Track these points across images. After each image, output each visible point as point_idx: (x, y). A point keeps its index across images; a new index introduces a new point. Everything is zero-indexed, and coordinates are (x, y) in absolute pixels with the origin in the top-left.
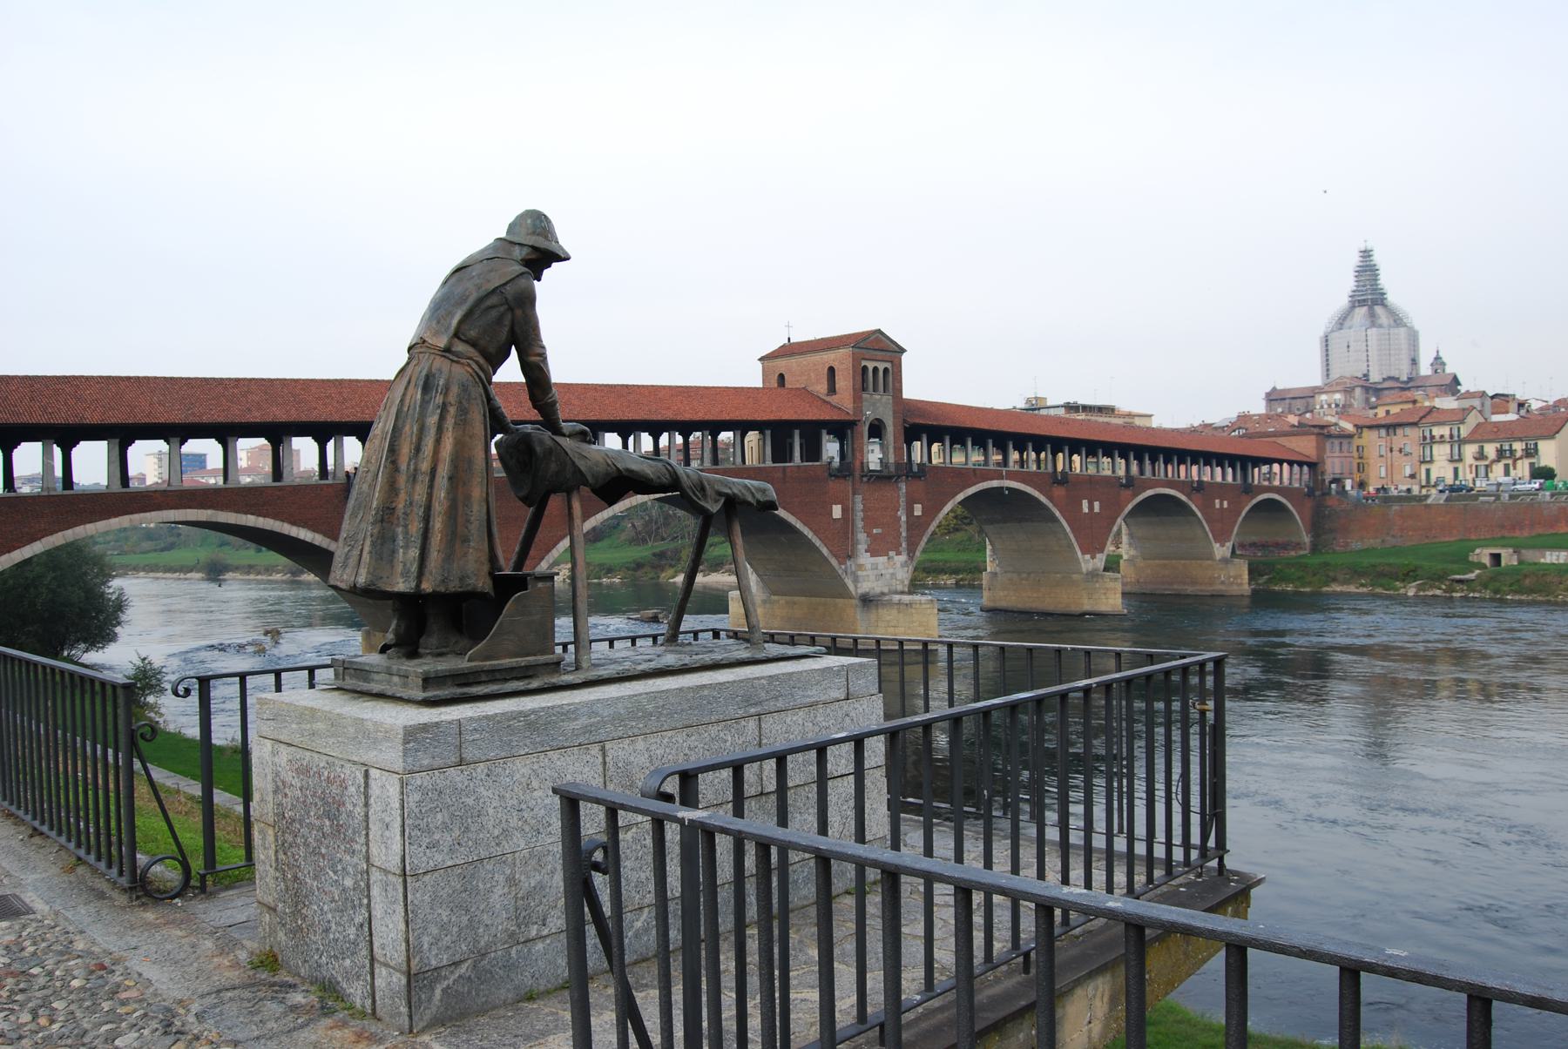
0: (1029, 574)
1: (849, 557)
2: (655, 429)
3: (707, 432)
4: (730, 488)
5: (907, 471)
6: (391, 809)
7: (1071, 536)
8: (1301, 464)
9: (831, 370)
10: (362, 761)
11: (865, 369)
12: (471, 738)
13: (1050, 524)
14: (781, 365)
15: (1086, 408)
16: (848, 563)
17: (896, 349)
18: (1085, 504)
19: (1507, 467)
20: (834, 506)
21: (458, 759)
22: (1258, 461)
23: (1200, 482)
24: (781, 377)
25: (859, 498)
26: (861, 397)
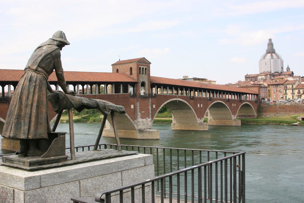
0: (184, 123)
1: (136, 119)
2: (83, 84)
3: (97, 85)
4: (113, 108)
5: (151, 96)
6: (21, 201)
7: (195, 113)
8: (254, 94)
9: (131, 68)
10: (12, 187)
11: (140, 68)
12: (43, 180)
13: (189, 110)
14: (118, 67)
15: (199, 79)
16: (135, 121)
17: (149, 63)
18: (199, 105)
20: (132, 105)
21: (40, 186)
22: (243, 94)
23: (228, 99)
24: (117, 70)
25: (138, 103)
26: (139, 76)
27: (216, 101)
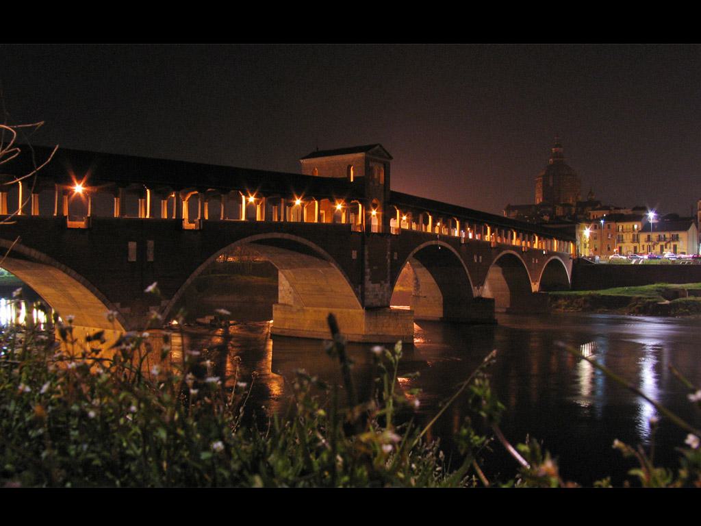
18: (475, 257)
19: (662, 247)
20: (353, 252)
25: (366, 247)
27: (504, 250)
